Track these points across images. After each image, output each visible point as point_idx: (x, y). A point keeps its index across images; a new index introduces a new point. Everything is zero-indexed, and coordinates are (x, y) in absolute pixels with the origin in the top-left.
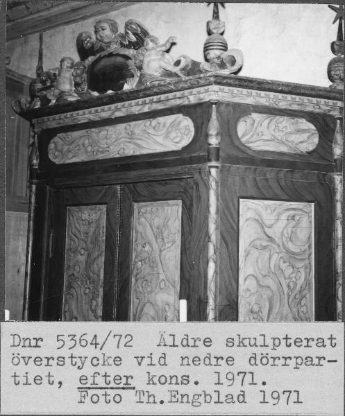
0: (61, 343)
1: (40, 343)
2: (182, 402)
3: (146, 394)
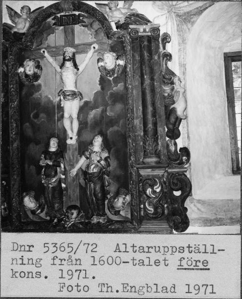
0: (47, 249)
1: (31, 249)
2: (131, 292)
3: (106, 285)
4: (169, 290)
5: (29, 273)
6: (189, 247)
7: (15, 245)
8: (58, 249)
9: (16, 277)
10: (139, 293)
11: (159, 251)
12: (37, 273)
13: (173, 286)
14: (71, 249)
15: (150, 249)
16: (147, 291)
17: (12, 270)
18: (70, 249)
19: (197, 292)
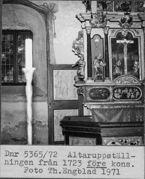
0: (26, 155)
1: (17, 155)
2: (68, 173)
3: (53, 169)
4: (91, 172)
7: (7, 152)
9: (114, 166)
10: (74, 174)
13: (94, 170)
14: (41, 155)
16: (79, 173)
19: (109, 173)
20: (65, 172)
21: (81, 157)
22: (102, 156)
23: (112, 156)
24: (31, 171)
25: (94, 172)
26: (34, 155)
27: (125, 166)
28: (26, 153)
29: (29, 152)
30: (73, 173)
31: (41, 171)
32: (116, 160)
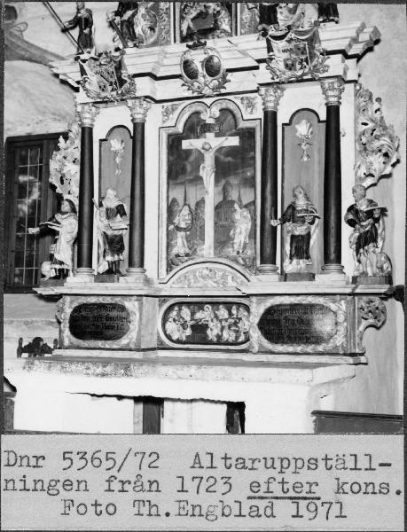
0: (68, 462)
1: (41, 462)
2: (193, 515)
3: (147, 504)
4: (261, 512)
5: (367, 485)
6: (326, 459)
7: (12, 456)
8: (89, 463)
9: (344, 493)
10: (209, 518)
11: (273, 465)
12: (383, 486)
15: (256, 463)
16: (223, 514)
17: (338, 479)
18: (111, 463)
20: (183, 512)
21: (331, 467)
22: (293, 462)
23: (321, 464)
24: (82, 509)
25: (269, 512)
26: (89, 461)
27: (374, 493)
28: (67, 456)
29: (75, 453)
30: (207, 515)
31: (112, 509)
32: (349, 476)
